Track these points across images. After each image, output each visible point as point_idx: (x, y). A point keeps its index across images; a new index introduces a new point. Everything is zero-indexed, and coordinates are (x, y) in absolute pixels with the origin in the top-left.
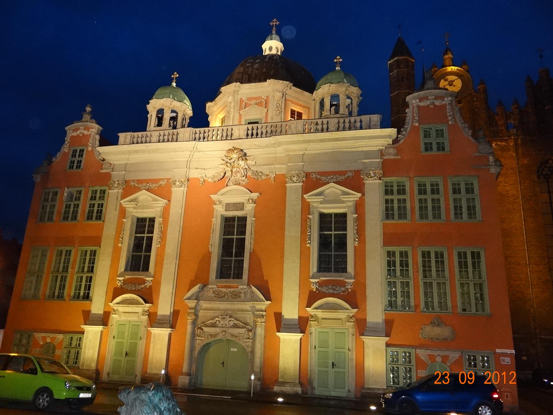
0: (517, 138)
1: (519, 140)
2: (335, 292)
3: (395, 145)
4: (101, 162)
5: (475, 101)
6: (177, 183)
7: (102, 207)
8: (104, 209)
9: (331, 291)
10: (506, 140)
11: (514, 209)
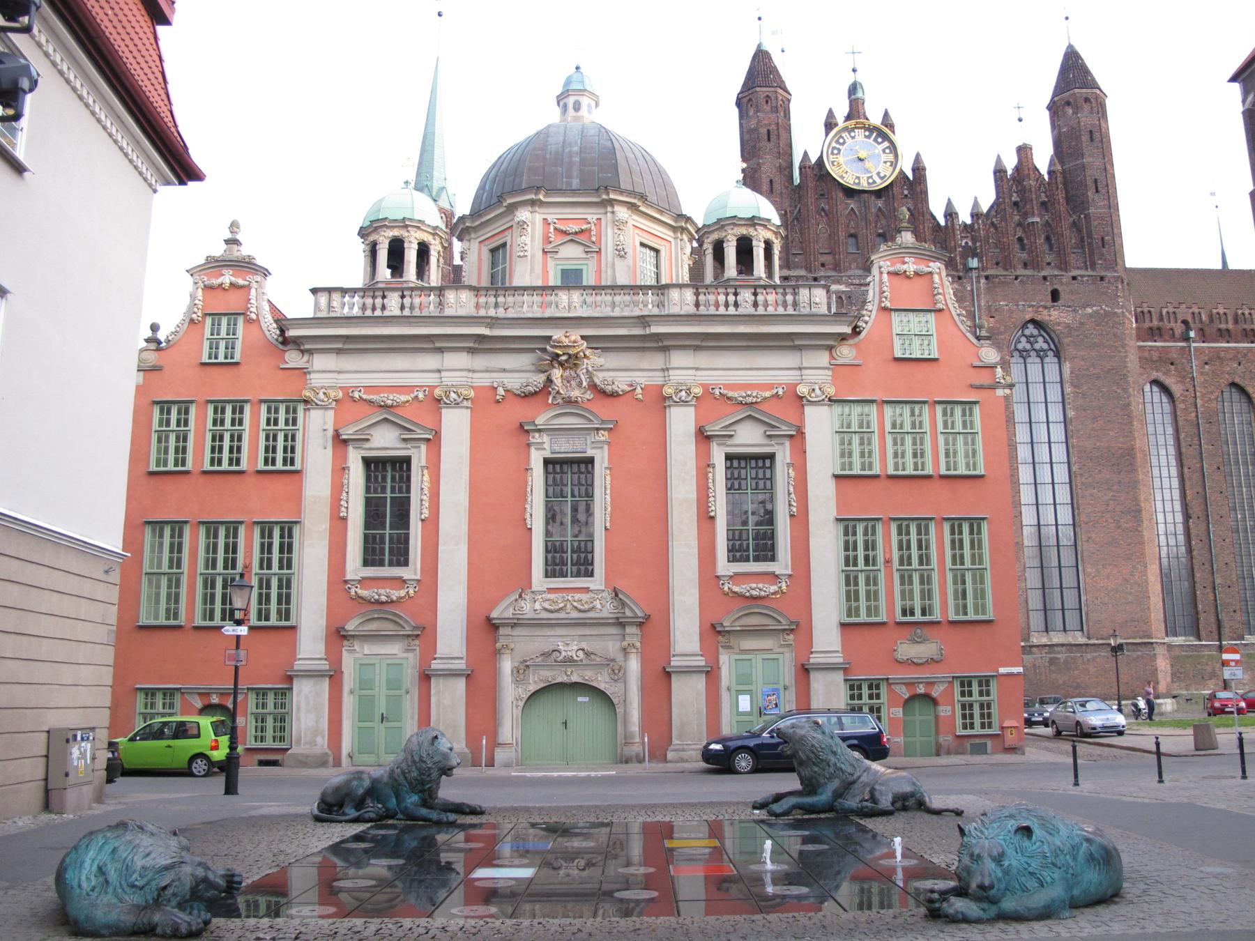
2: (763, 593)
4: (281, 347)
6: (453, 395)
9: (754, 593)
10: (960, 278)
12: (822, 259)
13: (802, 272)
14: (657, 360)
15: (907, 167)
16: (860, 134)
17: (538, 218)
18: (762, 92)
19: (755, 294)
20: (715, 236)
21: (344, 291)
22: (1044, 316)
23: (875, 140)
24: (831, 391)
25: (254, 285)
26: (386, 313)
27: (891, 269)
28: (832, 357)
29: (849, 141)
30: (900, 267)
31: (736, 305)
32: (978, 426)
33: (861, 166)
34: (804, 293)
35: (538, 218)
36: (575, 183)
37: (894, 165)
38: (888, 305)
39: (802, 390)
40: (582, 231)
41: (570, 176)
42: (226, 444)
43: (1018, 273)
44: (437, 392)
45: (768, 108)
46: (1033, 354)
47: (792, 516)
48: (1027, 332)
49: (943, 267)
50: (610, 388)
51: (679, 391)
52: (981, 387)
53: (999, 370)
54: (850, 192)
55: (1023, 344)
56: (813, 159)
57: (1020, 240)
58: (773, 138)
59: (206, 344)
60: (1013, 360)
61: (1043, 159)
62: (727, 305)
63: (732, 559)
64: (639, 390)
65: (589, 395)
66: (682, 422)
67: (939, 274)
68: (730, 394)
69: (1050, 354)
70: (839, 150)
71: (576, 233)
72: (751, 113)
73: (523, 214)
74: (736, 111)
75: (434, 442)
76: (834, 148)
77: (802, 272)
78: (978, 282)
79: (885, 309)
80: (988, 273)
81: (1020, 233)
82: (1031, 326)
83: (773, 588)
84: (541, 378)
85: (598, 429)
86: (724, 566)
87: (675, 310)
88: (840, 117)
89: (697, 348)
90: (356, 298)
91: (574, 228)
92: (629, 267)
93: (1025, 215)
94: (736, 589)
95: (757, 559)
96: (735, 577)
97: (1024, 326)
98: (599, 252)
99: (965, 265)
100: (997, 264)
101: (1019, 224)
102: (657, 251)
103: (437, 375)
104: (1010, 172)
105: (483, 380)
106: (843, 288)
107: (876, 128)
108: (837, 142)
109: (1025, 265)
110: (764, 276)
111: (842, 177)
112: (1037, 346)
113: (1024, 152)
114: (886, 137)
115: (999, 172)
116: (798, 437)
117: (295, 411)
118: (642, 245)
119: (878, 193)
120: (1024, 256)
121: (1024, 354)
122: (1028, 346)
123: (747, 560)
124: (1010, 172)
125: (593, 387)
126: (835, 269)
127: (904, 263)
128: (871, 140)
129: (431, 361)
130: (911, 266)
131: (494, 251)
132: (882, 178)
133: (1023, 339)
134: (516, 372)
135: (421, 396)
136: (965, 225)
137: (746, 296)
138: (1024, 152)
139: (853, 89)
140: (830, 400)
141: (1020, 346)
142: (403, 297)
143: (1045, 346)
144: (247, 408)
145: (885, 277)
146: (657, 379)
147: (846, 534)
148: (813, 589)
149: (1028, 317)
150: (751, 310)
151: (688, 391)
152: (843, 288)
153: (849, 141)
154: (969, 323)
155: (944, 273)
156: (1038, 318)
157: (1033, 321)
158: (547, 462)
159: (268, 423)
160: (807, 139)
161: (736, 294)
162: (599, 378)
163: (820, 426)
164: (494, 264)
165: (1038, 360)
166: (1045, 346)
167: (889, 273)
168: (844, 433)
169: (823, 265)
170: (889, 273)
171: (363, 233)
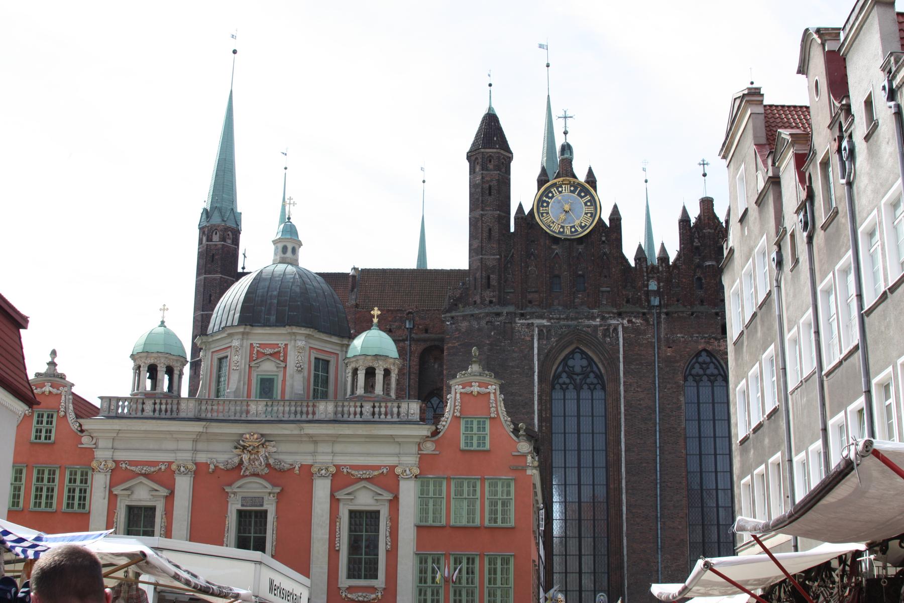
0: (660, 313)
1: (663, 316)
3: (434, 439)
5: (604, 242)
7: (85, 492)
8: (88, 495)
10: (644, 314)
11: (648, 430)
12: (530, 296)
13: (511, 309)
14: (310, 447)
16: (565, 189)
17: (247, 343)
19: (374, 407)
20: (353, 365)
21: (118, 399)
23: (579, 195)
24: (416, 471)
25: (63, 393)
26: (145, 414)
27: (463, 391)
28: (420, 449)
29: (557, 195)
30: (468, 389)
31: (361, 413)
32: (513, 496)
33: (565, 218)
34: (404, 406)
35: (247, 343)
36: (273, 318)
37: (593, 215)
38: (458, 414)
39: (398, 471)
40: (276, 353)
41: (269, 314)
42: (44, 493)
43: (695, 309)
44: (174, 467)
45: (491, 166)
46: (705, 378)
47: (387, 551)
48: (701, 360)
49: (498, 388)
50: (277, 467)
51: (320, 470)
52: (515, 469)
53: (529, 458)
54: (555, 240)
55: (697, 370)
56: (527, 211)
57: (699, 279)
58: (494, 192)
59: (34, 430)
60: (687, 384)
62: (355, 414)
63: (350, 576)
64: (297, 468)
65: (266, 471)
66: (322, 490)
67: (495, 393)
68: (353, 472)
69: (720, 378)
70: (548, 203)
71: (271, 355)
72: (477, 170)
73: (236, 343)
74: (467, 164)
75: (170, 498)
76: (545, 201)
77: (511, 309)
78: (659, 317)
79: (456, 417)
80: (670, 309)
81: (698, 274)
82: (704, 354)
83: (373, 596)
84: (236, 460)
85: (270, 493)
86: (344, 582)
87: (322, 417)
88: (551, 175)
89: (334, 442)
90: (126, 403)
91: (269, 351)
92: (303, 377)
93: (704, 259)
94: (349, 596)
95: (366, 578)
96: (350, 589)
97: (698, 354)
98: (285, 367)
99: (649, 301)
100: (678, 301)
101: (699, 266)
102: (328, 362)
103: (173, 455)
104: (693, 221)
105: (202, 458)
106: (545, 322)
107: (580, 184)
108: (547, 196)
109: (702, 302)
110: (381, 393)
111: (550, 226)
112: (708, 372)
113: (707, 204)
114: (587, 192)
115: (684, 221)
116: (394, 502)
117: (87, 475)
118: (316, 358)
119: (580, 240)
120: (700, 293)
121: (698, 379)
122: (701, 372)
123: (360, 577)
124: (693, 221)
125: (268, 465)
126: (539, 305)
127: (471, 386)
128: (575, 195)
129: (172, 445)
130: (475, 389)
131: (220, 360)
132: (582, 227)
133: (697, 366)
134: (221, 455)
135: (163, 467)
136: (653, 267)
137: (367, 408)
138: (707, 204)
140: (416, 477)
141: (694, 372)
142: (155, 404)
143: (716, 372)
144: (57, 473)
145: (458, 396)
146: (308, 460)
147: (421, 563)
148: (398, 598)
149: (700, 347)
150: (370, 418)
151: (327, 469)
152: (545, 322)
153: (557, 195)
154: (512, 426)
155: (498, 392)
156: (709, 348)
157: (705, 350)
158: (240, 513)
159: (70, 482)
160: (523, 192)
161: (361, 407)
162: (271, 461)
163: (408, 492)
164: (220, 368)
165: (709, 384)
166: (716, 372)
167: (461, 393)
168: (423, 498)
169: (530, 302)
170: (461, 393)
171: (133, 356)
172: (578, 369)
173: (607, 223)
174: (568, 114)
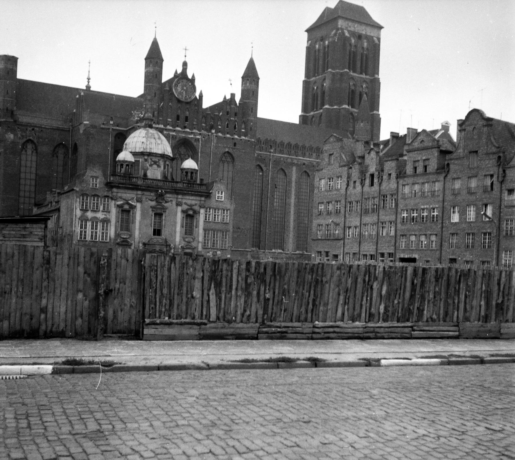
15: (197, 95)
18: (154, 58)
22: (231, 151)
46: (226, 162)
48: (225, 155)
61: (238, 99)
113: (233, 95)
138: (233, 95)
139: (185, 64)
172: (182, 153)
173: (198, 98)
174: (187, 48)
